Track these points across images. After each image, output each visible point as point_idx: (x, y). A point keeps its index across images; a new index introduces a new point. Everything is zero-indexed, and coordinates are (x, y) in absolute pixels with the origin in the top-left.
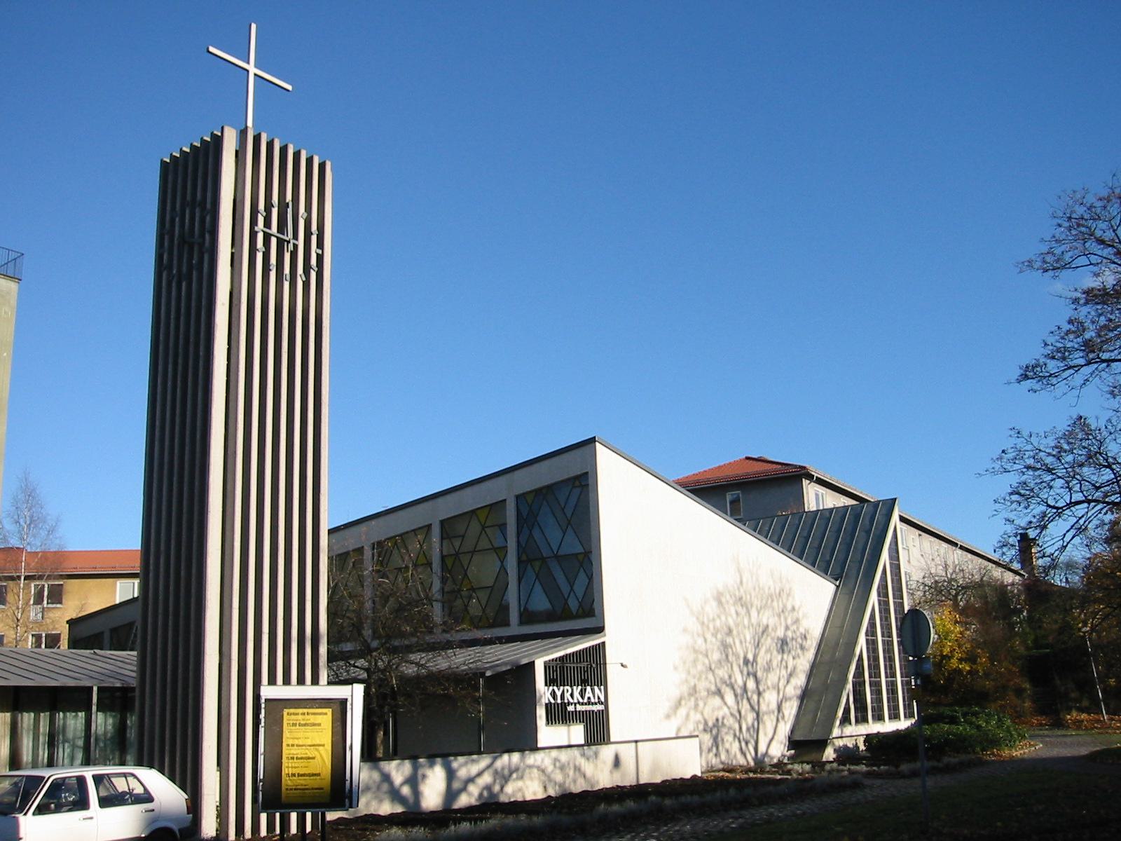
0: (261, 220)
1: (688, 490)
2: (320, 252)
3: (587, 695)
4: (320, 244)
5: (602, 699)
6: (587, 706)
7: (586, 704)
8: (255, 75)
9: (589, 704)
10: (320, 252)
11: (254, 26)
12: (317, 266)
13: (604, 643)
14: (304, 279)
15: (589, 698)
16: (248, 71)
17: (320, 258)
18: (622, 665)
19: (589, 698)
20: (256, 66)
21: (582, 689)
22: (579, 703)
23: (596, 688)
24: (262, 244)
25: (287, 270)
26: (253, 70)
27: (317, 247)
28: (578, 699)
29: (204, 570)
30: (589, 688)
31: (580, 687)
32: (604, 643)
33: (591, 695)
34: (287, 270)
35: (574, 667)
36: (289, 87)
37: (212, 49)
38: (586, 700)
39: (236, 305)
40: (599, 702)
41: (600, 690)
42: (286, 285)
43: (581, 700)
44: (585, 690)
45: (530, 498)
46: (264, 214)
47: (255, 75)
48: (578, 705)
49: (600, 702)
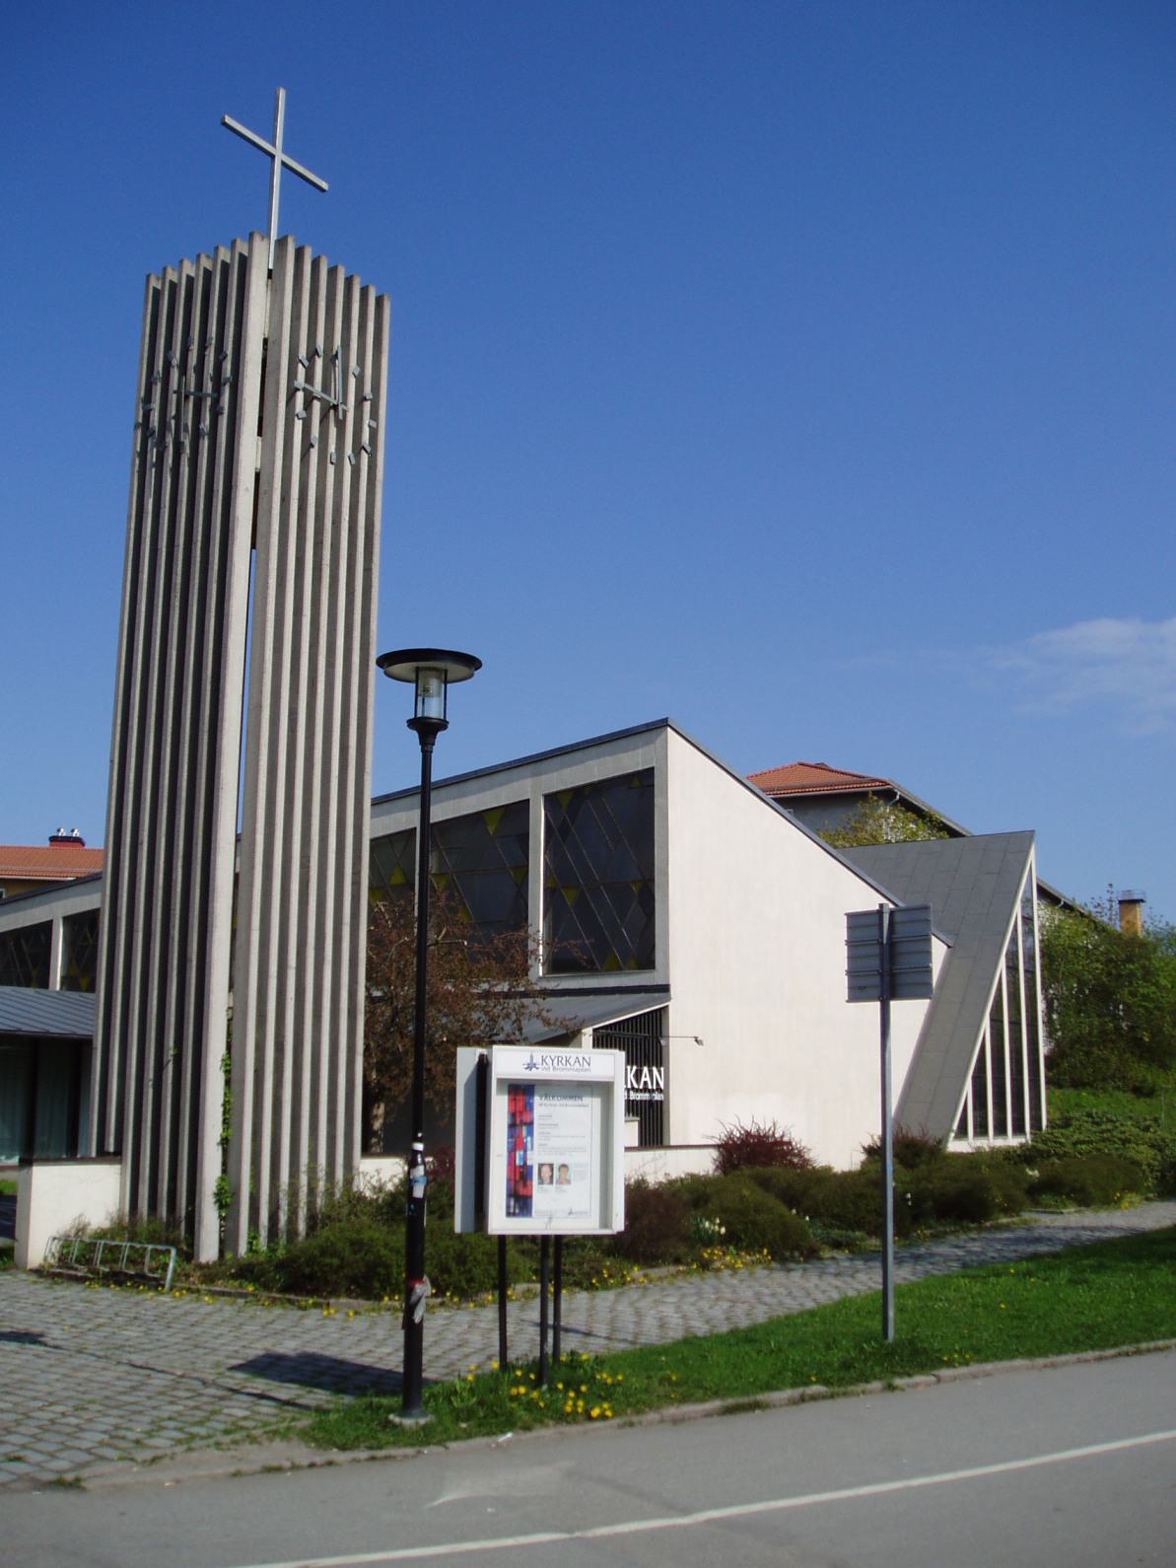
0: (301, 371)
1: (775, 799)
2: (374, 424)
3: (643, 1079)
4: (374, 415)
5: (662, 1086)
6: (642, 1094)
7: (641, 1091)
8: (284, 164)
9: (645, 1092)
10: (374, 424)
11: (282, 94)
12: (370, 445)
13: (667, 1007)
14: (353, 462)
15: (645, 1083)
16: (273, 157)
17: (374, 433)
18: (696, 1041)
19: (645, 1083)
20: (285, 151)
21: (637, 1071)
22: (633, 1088)
23: (654, 1069)
24: (302, 406)
25: (332, 448)
26: (280, 156)
27: (371, 418)
28: (632, 1084)
29: (657, 800)
30: (645, 1070)
31: (635, 1068)
32: (667, 1007)
33: (648, 1079)
34: (332, 448)
35: (636, 1031)
36: (324, 185)
37: (228, 120)
38: (641, 1087)
39: (266, 492)
40: (657, 1089)
41: (660, 1072)
42: (331, 469)
43: (636, 1086)
44: (641, 1071)
45: (565, 801)
46: (306, 363)
47: (284, 164)
48: (631, 1092)
49: (659, 1090)
